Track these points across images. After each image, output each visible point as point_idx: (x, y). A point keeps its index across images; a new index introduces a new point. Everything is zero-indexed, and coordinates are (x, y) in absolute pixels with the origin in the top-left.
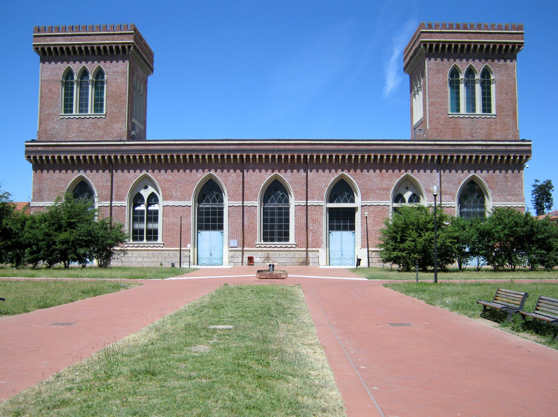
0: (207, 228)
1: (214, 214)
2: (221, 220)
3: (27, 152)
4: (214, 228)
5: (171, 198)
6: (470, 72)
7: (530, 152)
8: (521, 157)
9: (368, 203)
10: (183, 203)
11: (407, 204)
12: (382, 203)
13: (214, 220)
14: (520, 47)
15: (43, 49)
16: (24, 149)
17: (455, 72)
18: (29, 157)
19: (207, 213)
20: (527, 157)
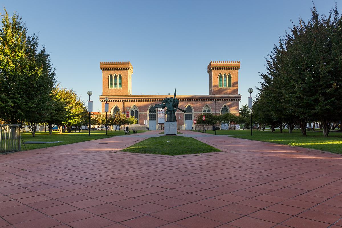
0: (152, 120)
1: (153, 116)
2: (155, 117)
3: (100, 99)
4: (153, 120)
5: (142, 112)
6: (225, 75)
7: (241, 98)
8: (238, 99)
9: (196, 112)
10: (145, 113)
11: (206, 113)
12: (200, 112)
13: (153, 117)
14: (239, 68)
15: (103, 69)
16: (99, 98)
17: (221, 76)
18: (101, 100)
19: (152, 116)
20: (240, 99)
